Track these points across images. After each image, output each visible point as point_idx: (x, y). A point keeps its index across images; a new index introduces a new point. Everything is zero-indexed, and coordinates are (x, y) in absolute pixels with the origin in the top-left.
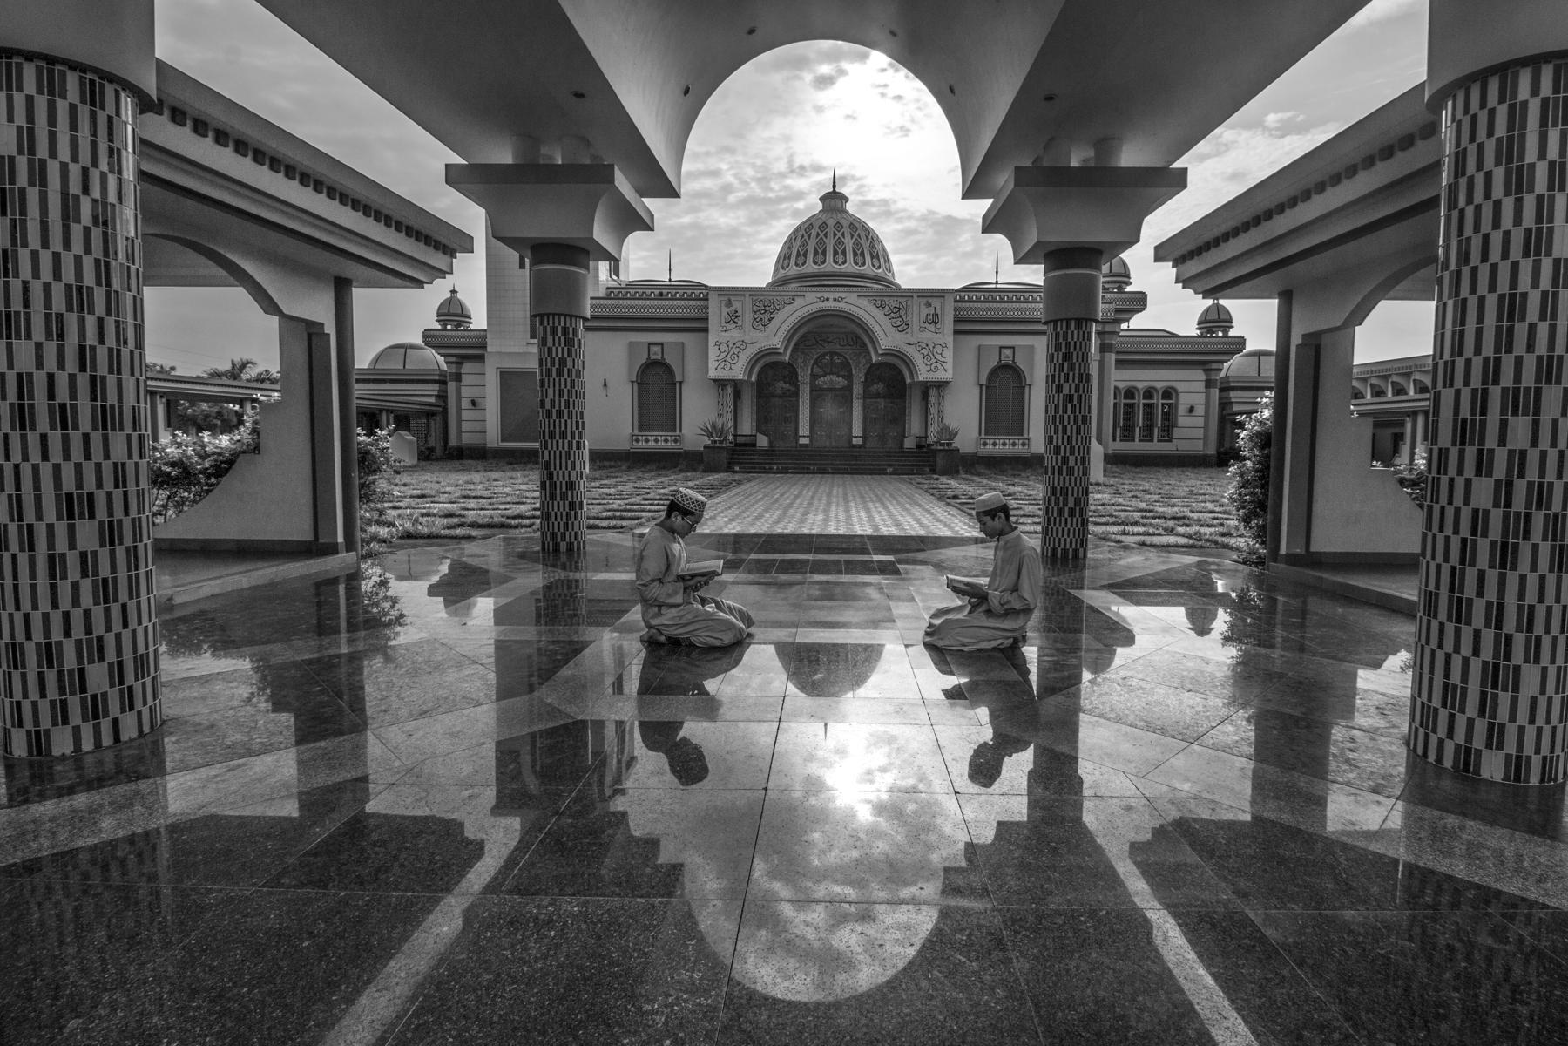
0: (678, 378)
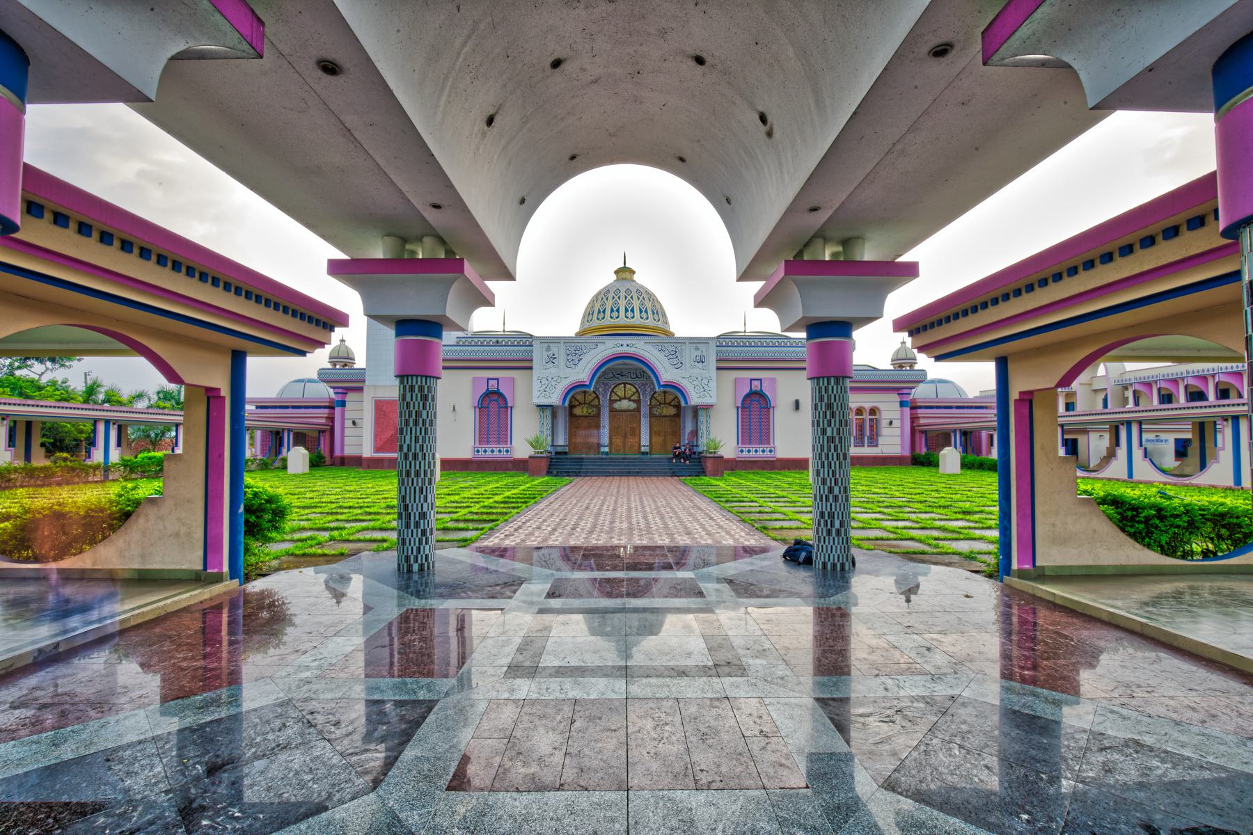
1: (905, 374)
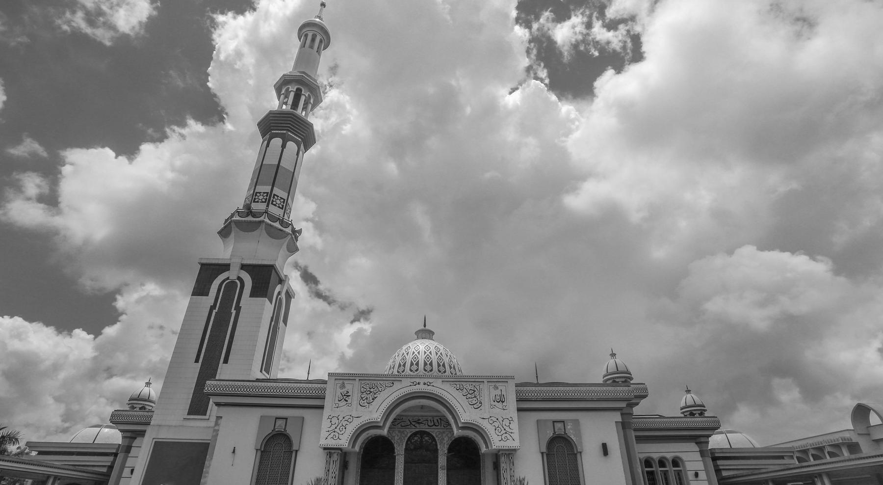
0: (295, 448)
1: (697, 421)
